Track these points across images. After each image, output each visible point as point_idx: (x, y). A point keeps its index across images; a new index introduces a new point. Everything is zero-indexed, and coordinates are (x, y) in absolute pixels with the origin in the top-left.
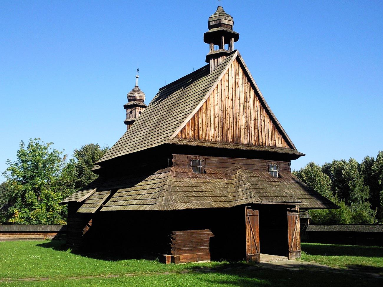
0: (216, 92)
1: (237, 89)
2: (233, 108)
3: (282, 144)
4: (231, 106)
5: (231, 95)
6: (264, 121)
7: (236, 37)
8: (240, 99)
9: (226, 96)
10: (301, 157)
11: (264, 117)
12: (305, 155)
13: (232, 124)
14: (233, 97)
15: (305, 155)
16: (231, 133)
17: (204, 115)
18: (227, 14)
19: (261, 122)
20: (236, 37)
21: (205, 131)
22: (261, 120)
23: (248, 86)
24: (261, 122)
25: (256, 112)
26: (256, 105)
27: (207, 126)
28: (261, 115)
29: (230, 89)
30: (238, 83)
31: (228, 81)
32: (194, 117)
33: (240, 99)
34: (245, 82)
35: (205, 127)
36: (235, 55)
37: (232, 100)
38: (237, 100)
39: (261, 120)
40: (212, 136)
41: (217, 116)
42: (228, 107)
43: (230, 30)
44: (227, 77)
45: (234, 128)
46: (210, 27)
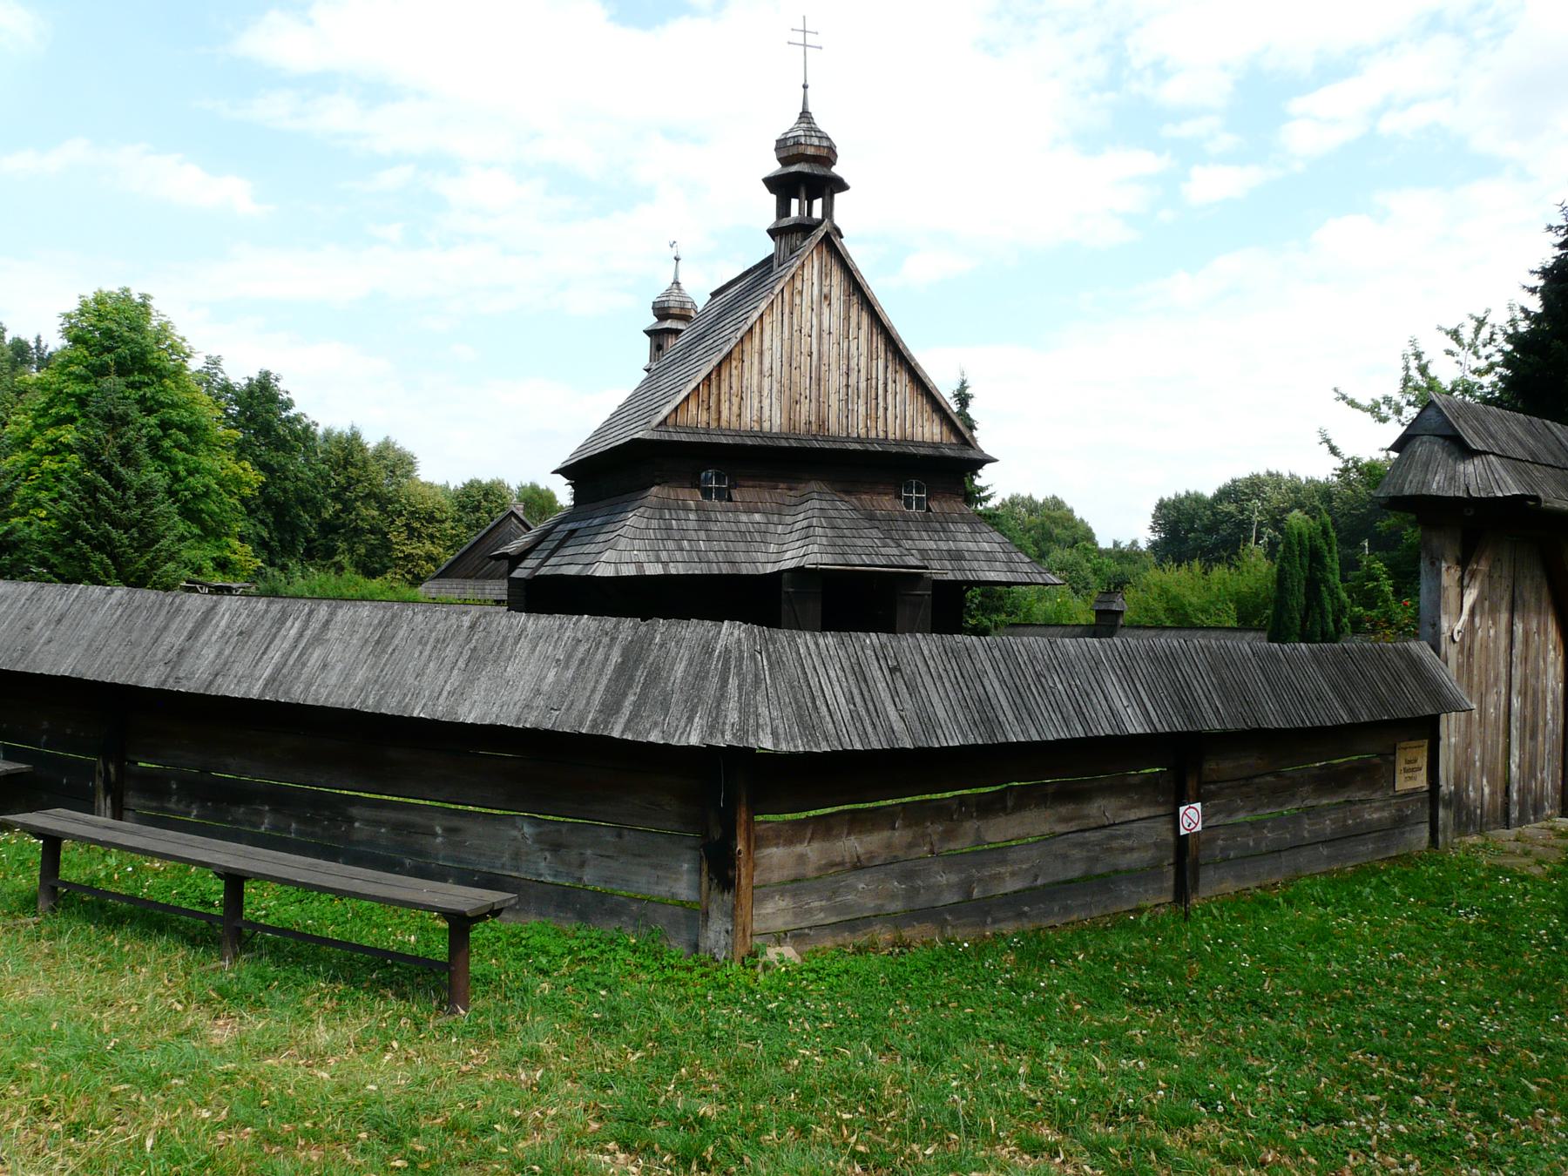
0: (767, 320)
1: (826, 310)
2: (810, 355)
3: (941, 433)
4: (805, 350)
5: (809, 324)
6: (895, 382)
7: (841, 185)
8: (830, 333)
9: (795, 328)
10: (987, 467)
11: (896, 372)
12: (996, 460)
13: (808, 391)
14: (814, 329)
15: (996, 460)
16: (805, 411)
17: (734, 372)
18: (820, 131)
19: (886, 384)
20: (840, 185)
21: (735, 409)
22: (886, 379)
23: (856, 301)
24: (886, 384)
25: (874, 362)
26: (874, 345)
27: (742, 398)
28: (887, 367)
29: (807, 310)
30: (827, 297)
31: (801, 293)
32: (709, 375)
33: (830, 333)
34: (847, 293)
35: (735, 400)
36: (820, 233)
37: (810, 336)
38: (825, 335)
39: (886, 379)
40: (755, 418)
41: (767, 374)
42: (798, 353)
43: (818, 170)
44: (798, 284)
45: (810, 400)
46: (785, 161)
